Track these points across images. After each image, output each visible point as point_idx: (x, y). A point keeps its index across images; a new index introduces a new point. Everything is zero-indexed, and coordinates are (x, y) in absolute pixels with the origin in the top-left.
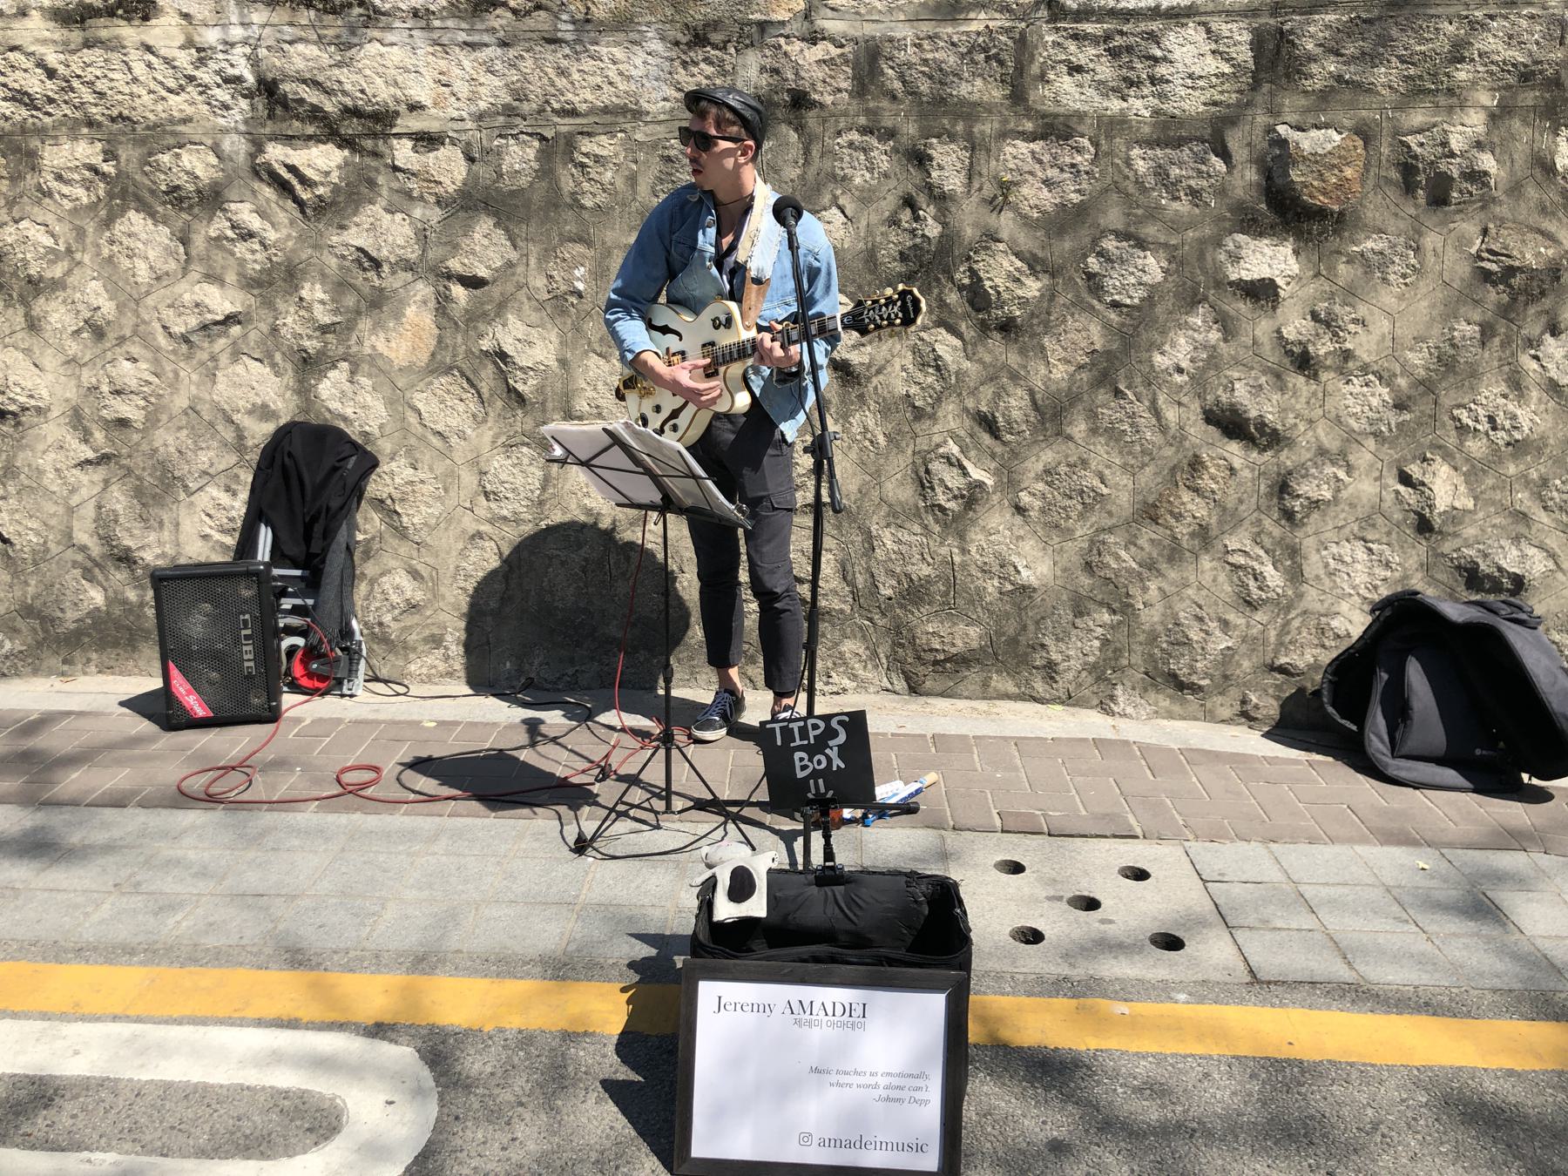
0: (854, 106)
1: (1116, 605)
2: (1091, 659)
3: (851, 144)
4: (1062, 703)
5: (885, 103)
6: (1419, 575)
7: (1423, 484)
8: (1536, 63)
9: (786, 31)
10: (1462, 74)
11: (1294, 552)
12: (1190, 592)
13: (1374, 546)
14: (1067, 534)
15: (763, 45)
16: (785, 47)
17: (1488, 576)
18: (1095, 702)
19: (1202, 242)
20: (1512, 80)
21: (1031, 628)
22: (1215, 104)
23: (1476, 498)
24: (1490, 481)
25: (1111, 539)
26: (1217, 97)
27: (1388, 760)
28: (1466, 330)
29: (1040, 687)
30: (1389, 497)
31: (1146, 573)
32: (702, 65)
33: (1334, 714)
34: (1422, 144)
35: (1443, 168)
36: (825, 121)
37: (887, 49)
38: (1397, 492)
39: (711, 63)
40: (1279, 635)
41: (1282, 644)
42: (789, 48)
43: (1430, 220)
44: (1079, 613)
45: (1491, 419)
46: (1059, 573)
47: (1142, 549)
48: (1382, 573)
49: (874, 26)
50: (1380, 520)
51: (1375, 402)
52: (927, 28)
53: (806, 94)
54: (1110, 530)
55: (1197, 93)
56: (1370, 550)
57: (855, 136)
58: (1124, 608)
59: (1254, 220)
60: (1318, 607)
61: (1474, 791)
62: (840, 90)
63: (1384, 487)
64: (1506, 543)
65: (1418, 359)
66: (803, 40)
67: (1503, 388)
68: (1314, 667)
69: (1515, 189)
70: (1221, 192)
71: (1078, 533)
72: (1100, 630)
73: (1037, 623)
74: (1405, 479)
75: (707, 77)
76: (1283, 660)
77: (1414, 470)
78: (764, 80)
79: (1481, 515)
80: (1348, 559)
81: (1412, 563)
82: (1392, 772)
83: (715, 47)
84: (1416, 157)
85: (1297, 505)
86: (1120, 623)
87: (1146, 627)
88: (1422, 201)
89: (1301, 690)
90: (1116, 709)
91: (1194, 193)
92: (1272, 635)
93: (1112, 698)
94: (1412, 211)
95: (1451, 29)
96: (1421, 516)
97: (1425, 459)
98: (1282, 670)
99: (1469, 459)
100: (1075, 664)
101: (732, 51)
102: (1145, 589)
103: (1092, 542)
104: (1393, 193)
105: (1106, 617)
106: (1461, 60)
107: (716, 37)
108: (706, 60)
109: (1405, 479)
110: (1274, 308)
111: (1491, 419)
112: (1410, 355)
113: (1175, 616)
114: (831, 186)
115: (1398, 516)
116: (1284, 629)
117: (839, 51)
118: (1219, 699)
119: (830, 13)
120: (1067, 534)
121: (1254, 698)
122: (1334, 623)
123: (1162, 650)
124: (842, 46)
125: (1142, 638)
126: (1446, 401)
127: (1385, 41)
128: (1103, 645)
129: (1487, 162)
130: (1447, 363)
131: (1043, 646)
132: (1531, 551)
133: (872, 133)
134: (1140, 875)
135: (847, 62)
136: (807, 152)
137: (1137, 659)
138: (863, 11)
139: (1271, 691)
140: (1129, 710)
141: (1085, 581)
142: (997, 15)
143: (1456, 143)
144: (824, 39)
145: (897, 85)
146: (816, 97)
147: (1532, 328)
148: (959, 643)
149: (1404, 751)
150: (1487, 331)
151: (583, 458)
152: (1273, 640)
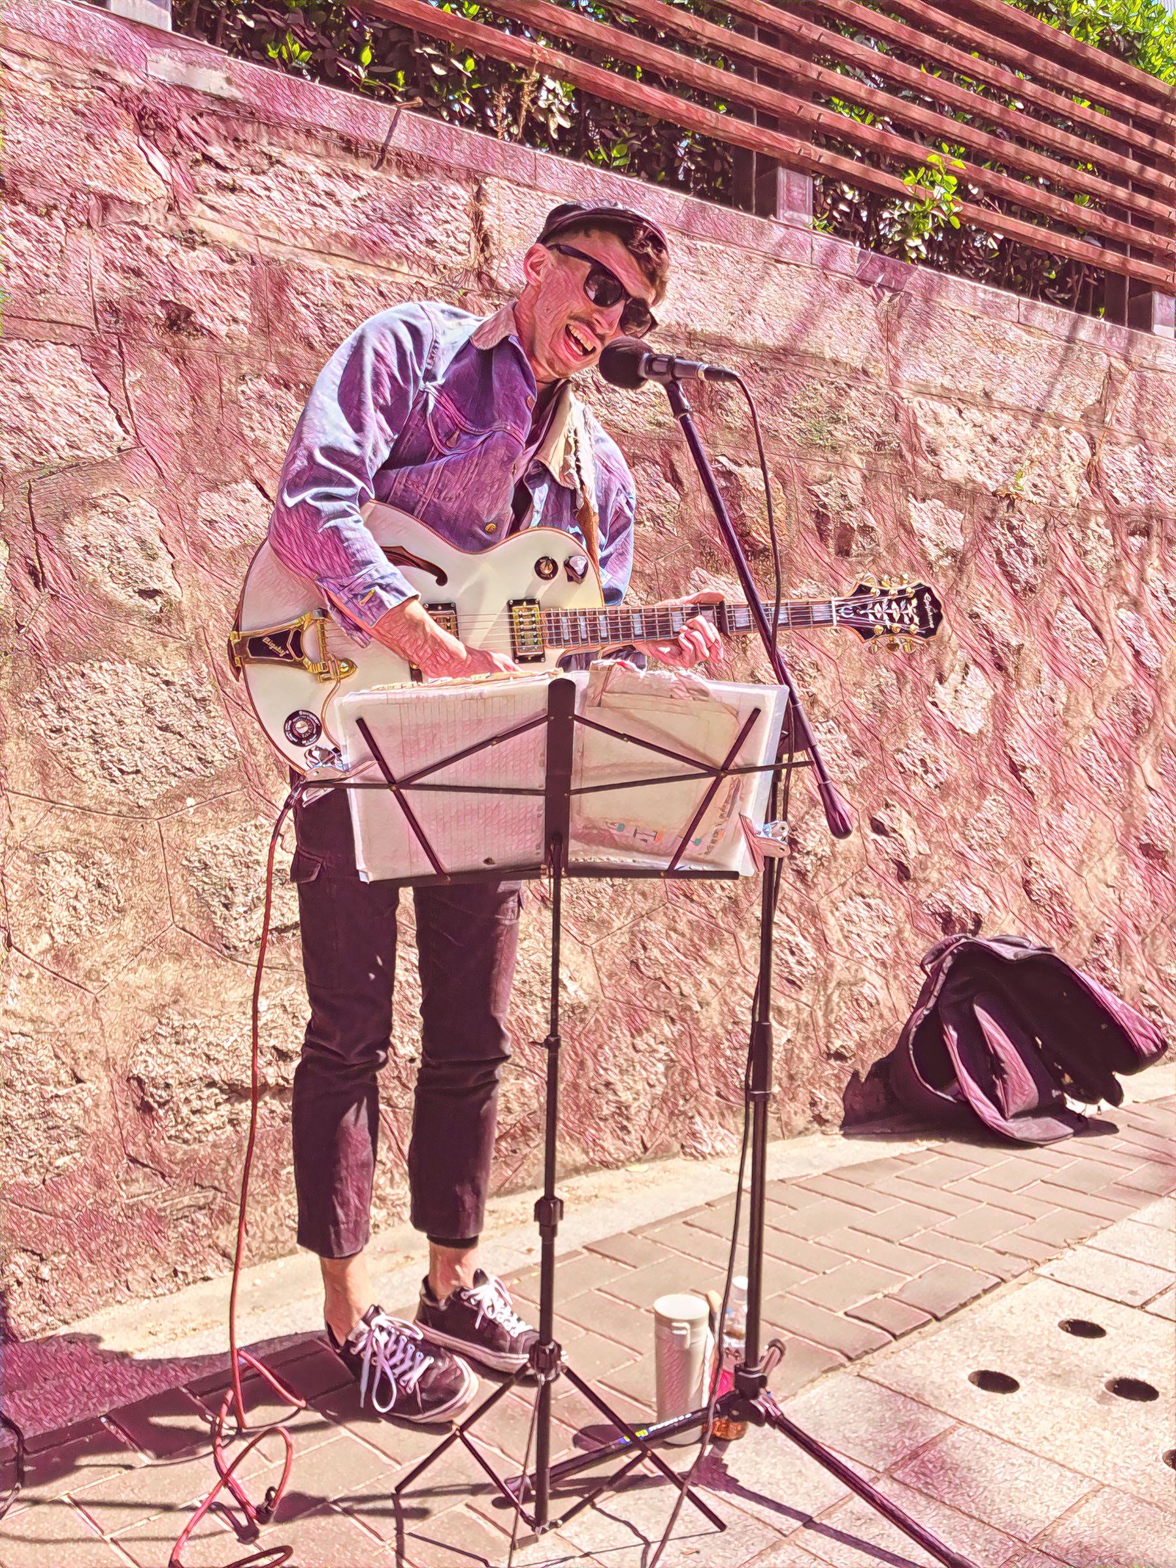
0: (259, 344)
1: (673, 1012)
2: (659, 1090)
3: (261, 397)
4: (639, 1160)
5: (300, 351)
6: (908, 926)
7: (895, 831)
8: (885, 434)
9: (144, 220)
10: (841, 434)
11: (815, 915)
12: (738, 980)
13: (872, 901)
14: (603, 925)
15: (106, 230)
16: (146, 241)
17: (960, 918)
18: (676, 1147)
19: (674, 572)
20: (870, 447)
21: (590, 1063)
22: (659, 424)
23: (929, 842)
24: (933, 825)
25: (652, 926)
26: (660, 418)
27: (1002, 1122)
28: (889, 677)
29: (609, 1143)
30: (871, 847)
31: (694, 966)
32: (10, 232)
33: (905, 1096)
34: (826, 495)
35: (846, 519)
36: (220, 357)
37: (297, 278)
38: (875, 841)
39: (26, 233)
40: (826, 1016)
41: (830, 1025)
42: (154, 245)
43: (843, 568)
44: (636, 1032)
45: (923, 761)
46: (606, 981)
47: (683, 935)
48: (883, 929)
49: (274, 246)
50: (870, 873)
51: (839, 747)
52: (343, 267)
53: (189, 313)
54: (649, 915)
55: (641, 409)
56: (869, 905)
57: (263, 385)
58: (683, 1014)
59: (711, 554)
60: (846, 976)
61: (1075, 1134)
62: (235, 320)
63: (864, 837)
64: (958, 883)
65: (860, 703)
66: (172, 237)
67: (922, 734)
68: (862, 1046)
69: (891, 547)
70: (681, 520)
71: (616, 924)
72: (662, 1049)
73: (595, 1055)
74: (878, 828)
75: (19, 253)
76: (836, 1044)
77: (881, 815)
78: (116, 284)
79: (936, 858)
80: (856, 919)
81: (901, 915)
82: (1018, 1135)
83: (32, 208)
84: (824, 506)
85: (807, 863)
86: (682, 1033)
87: (708, 1034)
88: (832, 550)
89: (856, 1075)
90: (706, 1149)
91: (654, 518)
92: (820, 1014)
93: (693, 1135)
94: (827, 559)
95: (824, 391)
96: (900, 865)
97: (887, 806)
98: (839, 1056)
99: (916, 802)
100: (644, 1100)
101: (62, 226)
102: (698, 985)
103: (632, 933)
104: (813, 541)
105: (667, 1030)
106: (837, 421)
107: (29, 192)
108: (16, 225)
109: (878, 828)
110: (744, 650)
111: (923, 761)
112: (855, 700)
113: (732, 1012)
114: (240, 449)
115: (882, 867)
116: (827, 1012)
117: (225, 267)
118: (791, 1107)
119: (209, 213)
120: (603, 925)
121: (819, 1094)
122: (866, 990)
123: (727, 1058)
124: (232, 261)
125: (706, 1048)
126: (890, 748)
127: (779, 391)
128: (667, 1068)
129: (872, 522)
130: (880, 708)
131: (608, 1085)
132: (975, 889)
133: (287, 386)
134: (1083, 1329)
135: (243, 284)
136: (196, 396)
137: (707, 1077)
138: (256, 223)
139: (832, 1083)
140: (719, 1146)
141: (635, 985)
142: (426, 276)
143: (854, 500)
144: (205, 244)
145: (314, 331)
146: (206, 322)
147: (930, 677)
148: (515, 1106)
149: (1013, 1109)
150: (900, 676)
151: (398, 773)
152: (821, 1022)
